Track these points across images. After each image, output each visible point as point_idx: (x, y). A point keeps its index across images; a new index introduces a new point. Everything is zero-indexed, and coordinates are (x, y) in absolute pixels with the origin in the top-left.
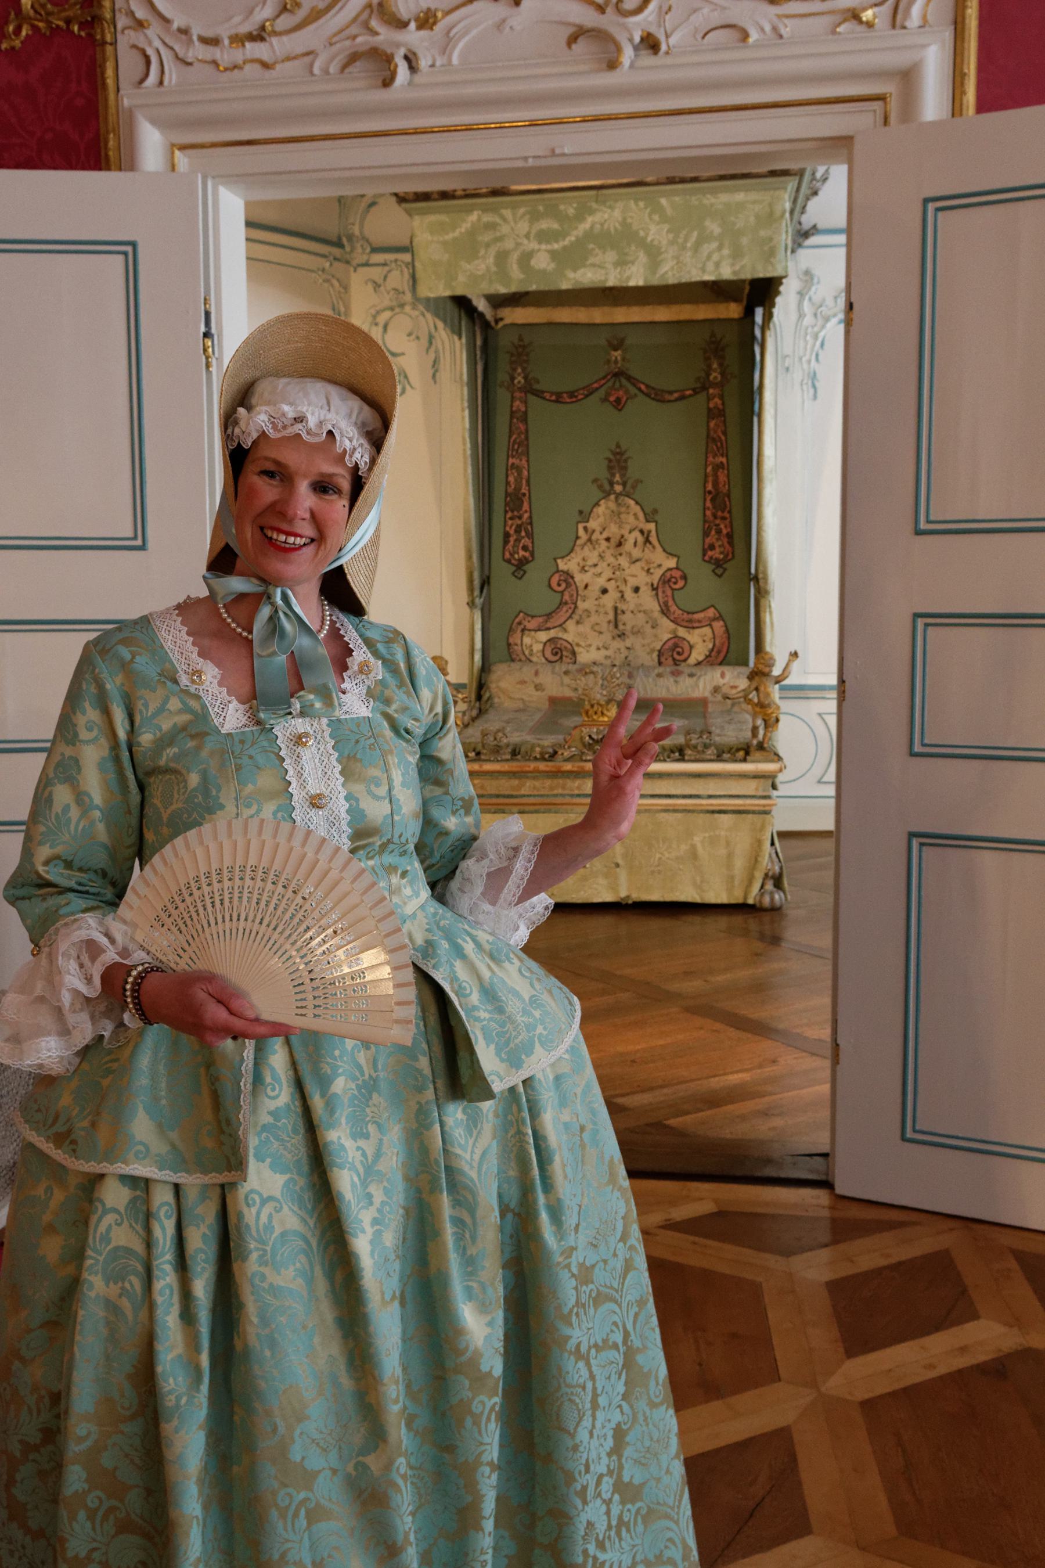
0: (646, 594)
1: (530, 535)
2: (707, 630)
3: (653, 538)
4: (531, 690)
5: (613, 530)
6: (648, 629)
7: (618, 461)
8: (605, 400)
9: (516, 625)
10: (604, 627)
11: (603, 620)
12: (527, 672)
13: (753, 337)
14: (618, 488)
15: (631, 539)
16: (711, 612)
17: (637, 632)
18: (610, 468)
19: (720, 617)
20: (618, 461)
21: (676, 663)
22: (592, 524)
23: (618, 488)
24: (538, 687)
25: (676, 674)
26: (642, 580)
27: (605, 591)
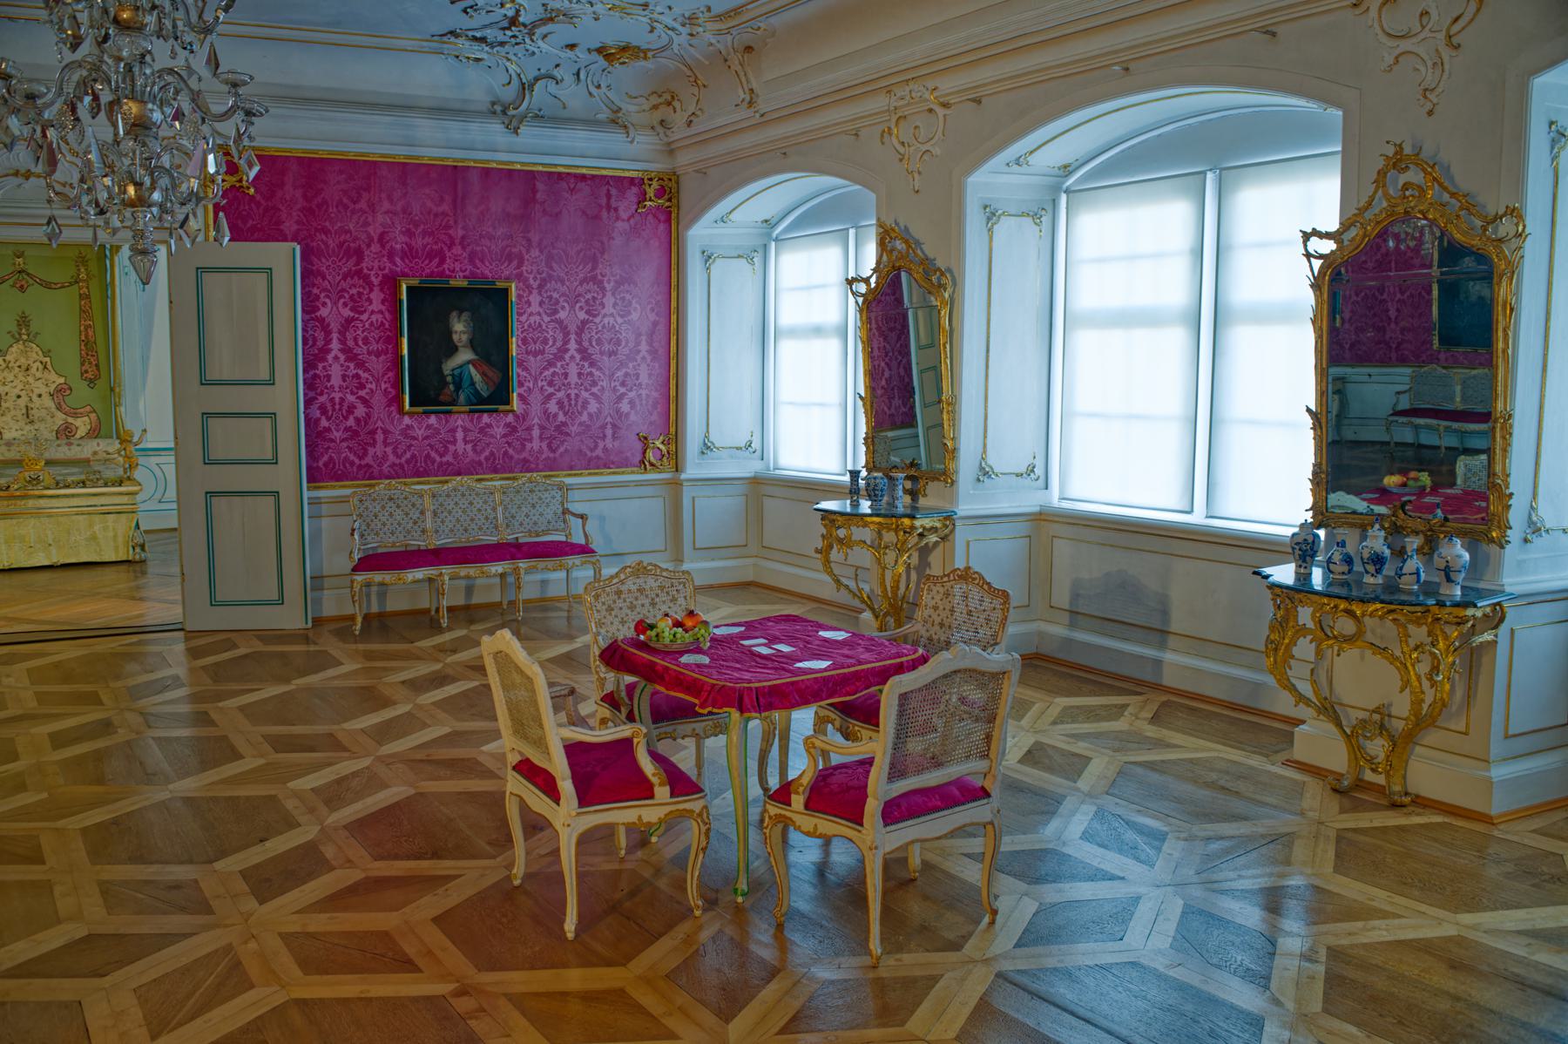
3: (49, 366)
7: (23, 321)
10: (20, 417)
11: (19, 414)
15: (35, 366)
16: (88, 408)
17: (42, 420)
19: (94, 411)
20: (23, 321)
21: (67, 437)
23: (25, 337)
25: (69, 444)
27: (19, 397)
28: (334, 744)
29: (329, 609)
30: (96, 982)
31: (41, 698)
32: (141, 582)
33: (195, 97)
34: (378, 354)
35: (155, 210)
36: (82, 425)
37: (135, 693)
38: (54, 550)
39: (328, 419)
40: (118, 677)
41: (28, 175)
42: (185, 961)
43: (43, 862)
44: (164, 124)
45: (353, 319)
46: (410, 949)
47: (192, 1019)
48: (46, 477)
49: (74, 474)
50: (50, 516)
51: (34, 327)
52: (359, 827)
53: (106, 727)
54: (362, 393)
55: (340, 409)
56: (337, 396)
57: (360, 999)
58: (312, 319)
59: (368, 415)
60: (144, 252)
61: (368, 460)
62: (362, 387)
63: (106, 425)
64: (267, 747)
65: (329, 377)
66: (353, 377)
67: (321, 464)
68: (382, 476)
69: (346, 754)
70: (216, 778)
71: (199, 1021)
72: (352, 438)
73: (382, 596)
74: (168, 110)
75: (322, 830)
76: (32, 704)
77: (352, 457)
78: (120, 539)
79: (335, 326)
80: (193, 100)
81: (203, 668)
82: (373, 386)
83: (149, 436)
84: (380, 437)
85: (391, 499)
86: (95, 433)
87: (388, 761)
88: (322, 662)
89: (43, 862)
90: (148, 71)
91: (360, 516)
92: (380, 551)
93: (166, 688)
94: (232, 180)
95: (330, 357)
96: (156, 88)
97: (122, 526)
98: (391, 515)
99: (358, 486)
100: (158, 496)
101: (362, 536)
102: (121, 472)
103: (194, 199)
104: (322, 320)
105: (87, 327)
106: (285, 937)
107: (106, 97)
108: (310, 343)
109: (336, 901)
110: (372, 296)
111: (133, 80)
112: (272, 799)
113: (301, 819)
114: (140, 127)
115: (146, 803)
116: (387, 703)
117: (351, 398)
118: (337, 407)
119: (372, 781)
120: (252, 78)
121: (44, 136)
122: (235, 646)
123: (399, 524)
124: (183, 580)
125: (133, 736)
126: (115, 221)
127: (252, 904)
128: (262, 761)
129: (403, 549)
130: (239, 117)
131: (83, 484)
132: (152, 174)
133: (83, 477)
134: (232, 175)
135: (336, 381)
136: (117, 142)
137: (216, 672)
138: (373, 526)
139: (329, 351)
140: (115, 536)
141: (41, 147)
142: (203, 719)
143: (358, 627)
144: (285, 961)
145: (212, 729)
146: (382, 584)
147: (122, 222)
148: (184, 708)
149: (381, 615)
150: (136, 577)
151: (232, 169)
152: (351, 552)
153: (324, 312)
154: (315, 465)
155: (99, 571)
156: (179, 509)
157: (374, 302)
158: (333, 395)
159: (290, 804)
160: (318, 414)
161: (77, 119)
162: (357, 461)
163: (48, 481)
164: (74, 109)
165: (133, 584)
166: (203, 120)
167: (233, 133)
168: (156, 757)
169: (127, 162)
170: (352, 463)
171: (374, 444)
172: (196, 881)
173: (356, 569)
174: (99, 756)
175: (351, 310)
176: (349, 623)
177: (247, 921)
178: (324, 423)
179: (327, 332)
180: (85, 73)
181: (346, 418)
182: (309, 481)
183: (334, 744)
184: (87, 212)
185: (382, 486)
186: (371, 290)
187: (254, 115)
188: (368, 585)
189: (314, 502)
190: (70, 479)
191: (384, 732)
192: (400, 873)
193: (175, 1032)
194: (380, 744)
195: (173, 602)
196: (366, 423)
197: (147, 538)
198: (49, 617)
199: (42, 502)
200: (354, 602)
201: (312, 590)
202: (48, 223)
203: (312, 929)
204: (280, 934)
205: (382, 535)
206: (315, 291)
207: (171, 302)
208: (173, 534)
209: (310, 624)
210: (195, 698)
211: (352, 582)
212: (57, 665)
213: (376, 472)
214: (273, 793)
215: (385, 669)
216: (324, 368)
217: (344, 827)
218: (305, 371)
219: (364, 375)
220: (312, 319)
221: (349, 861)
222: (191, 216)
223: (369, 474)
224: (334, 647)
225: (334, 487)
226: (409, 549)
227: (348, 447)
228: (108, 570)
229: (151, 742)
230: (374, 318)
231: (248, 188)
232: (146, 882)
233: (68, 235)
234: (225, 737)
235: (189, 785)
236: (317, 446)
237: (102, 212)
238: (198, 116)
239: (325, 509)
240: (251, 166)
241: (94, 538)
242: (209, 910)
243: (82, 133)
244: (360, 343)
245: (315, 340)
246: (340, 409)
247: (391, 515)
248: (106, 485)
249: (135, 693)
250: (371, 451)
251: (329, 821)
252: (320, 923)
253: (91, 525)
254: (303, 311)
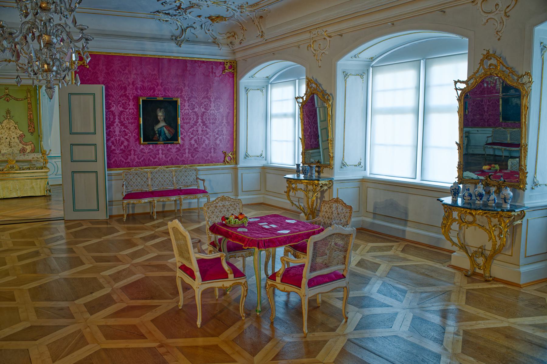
3: (17, 128)
7: (8, 112)
10: (7, 145)
11: (7, 144)
15: (12, 128)
16: (31, 142)
17: (15, 146)
19: (33, 143)
20: (8, 112)
21: (24, 152)
23: (9, 118)
25: (24, 155)
27: (7, 138)
28: (117, 259)
29: (115, 212)
30: (34, 342)
31: (14, 243)
32: (49, 203)
33: (68, 34)
34: (132, 123)
35: (54, 73)
36: (29, 148)
37: (47, 242)
38: (19, 192)
39: (115, 146)
40: (41, 236)
41: (10, 61)
42: (64, 335)
43: (15, 301)
44: (57, 43)
45: (123, 111)
46: (143, 331)
47: (67, 355)
48: (16, 166)
49: (26, 165)
50: (17, 180)
51: (12, 114)
52: (125, 288)
53: (37, 253)
54: (126, 137)
55: (119, 143)
56: (118, 138)
57: (126, 348)
58: (109, 111)
59: (129, 145)
60: (50, 88)
61: (129, 160)
62: (126, 135)
63: (37, 148)
64: (93, 261)
65: (115, 132)
66: (123, 131)
67: (112, 162)
68: (133, 166)
69: (121, 263)
70: (75, 271)
71: (69, 356)
72: (123, 153)
73: (133, 208)
74: (59, 39)
75: (112, 289)
76: (11, 245)
77: (123, 159)
78: (42, 188)
79: (117, 114)
80: (67, 35)
81: (71, 233)
82: (130, 135)
83: (52, 152)
84: (132, 152)
85: (136, 174)
86: (33, 151)
87: (135, 265)
88: (112, 231)
89: (15, 301)
90: (52, 25)
91: (126, 180)
92: (133, 192)
93: (58, 240)
94: (81, 63)
95: (115, 124)
96: (54, 31)
97: (43, 183)
98: (136, 179)
99: (125, 170)
100: (55, 173)
101: (126, 187)
102: (42, 164)
103: (68, 70)
104: (112, 112)
105: (30, 114)
106: (99, 327)
107: (37, 34)
108: (108, 119)
109: (117, 314)
110: (130, 103)
111: (46, 28)
112: (95, 278)
113: (105, 286)
114: (49, 44)
115: (51, 280)
116: (135, 245)
117: (123, 139)
118: (118, 142)
119: (130, 272)
120: (88, 27)
121: (16, 47)
122: (82, 225)
123: (139, 183)
124: (64, 202)
125: (47, 257)
126: (40, 77)
127: (88, 315)
128: (91, 265)
129: (141, 191)
130: (83, 41)
131: (29, 169)
132: (53, 61)
133: (29, 166)
134: (81, 61)
135: (117, 133)
136: (41, 50)
137: (75, 234)
138: (130, 183)
139: (115, 122)
140: (40, 187)
141: (14, 51)
142: (71, 251)
143: (125, 218)
144: (99, 335)
145: (74, 254)
146: (133, 204)
147: (43, 77)
148: (64, 247)
149: (133, 215)
150: (48, 201)
151: (81, 59)
152: (122, 193)
153: (113, 109)
154: (110, 162)
155: (35, 199)
156: (62, 177)
157: (131, 105)
158: (116, 138)
159: (101, 280)
160: (111, 144)
161: (27, 42)
162: (125, 161)
163: (17, 168)
164: (26, 38)
165: (46, 204)
166: (71, 42)
167: (81, 46)
168: (54, 264)
169: (44, 56)
170: (123, 162)
171: (130, 155)
172: (68, 307)
173: (124, 198)
174: (34, 264)
175: (123, 108)
176: (122, 217)
177: (86, 321)
178: (113, 147)
179: (114, 116)
180: (30, 25)
181: (121, 146)
182: (108, 168)
183: (117, 259)
184: (30, 74)
185: (133, 170)
186: (130, 101)
187: (89, 40)
188: (128, 204)
189: (110, 175)
190: (24, 167)
191: (134, 255)
192: (140, 305)
193: (61, 360)
194: (133, 259)
195: (60, 210)
196: (128, 148)
197: (51, 187)
198: (17, 215)
199: (15, 175)
200: (123, 210)
201: (109, 206)
202: (17, 78)
203: (109, 324)
204: (98, 326)
205: (133, 186)
206: (110, 101)
207: (60, 105)
208: (61, 186)
209: (108, 218)
210: (68, 243)
211: (123, 203)
212: (20, 232)
213: (131, 164)
214: (95, 276)
215: (134, 233)
216: (113, 128)
217: (120, 288)
218: (106, 129)
219: (127, 131)
220: (109, 111)
221: (122, 300)
222: (67, 75)
223: (129, 165)
224: (116, 226)
225: (116, 170)
226: (143, 191)
227: (121, 156)
228: (38, 199)
229: (53, 259)
230: (130, 111)
231: (87, 66)
232: (51, 308)
233: (24, 82)
234: (79, 257)
235: (66, 274)
236: (111, 155)
237: (36, 74)
238: (69, 40)
239: (113, 177)
240: (87, 58)
241: (33, 188)
242: (73, 317)
243: (29, 46)
244: (126, 119)
245: (110, 118)
246: (119, 143)
247: (136, 179)
248: (37, 169)
249: (47, 242)
250: (129, 157)
251: (115, 286)
252: (112, 322)
253: (32, 183)
254: (106, 108)
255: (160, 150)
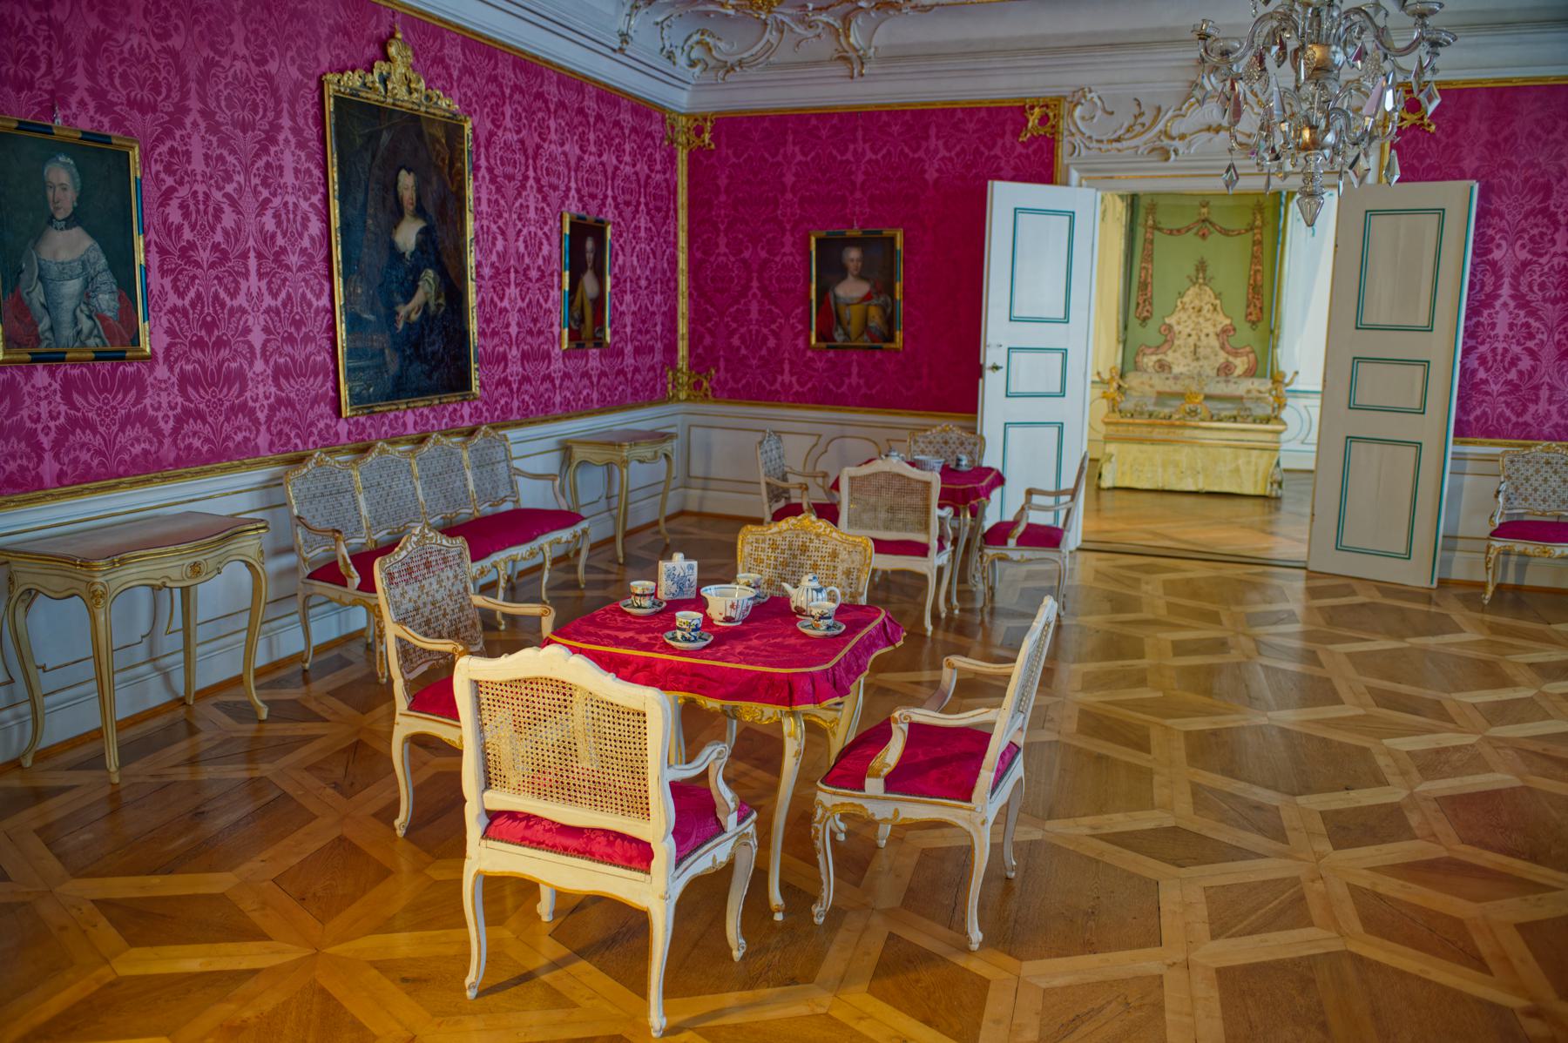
0: (1212, 336)
1: (1150, 304)
2: (1245, 359)
3: (1219, 308)
4: (1147, 388)
5: (1197, 303)
6: (1213, 357)
7: (1201, 267)
8: (1196, 234)
9: (1140, 352)
10: (1188, 354)
11: (1188, 350)
12: (1145, 377)
13: (1281, 203)
14: (1201, 281)
15: (1206, 308)
16: (1248, 349)
17: (1206, 358)
18: (1197, 270)
19: (1253, 352)
20: (1201, 267)
21: (1227, 375)
22: (1186, 299)
23: (1201, 281)
24: (1151, 386)
25: (1227, 381)
26: (1211, 330)
27: (1190, 335)
28: (1439, 712)
29: (1459, 572)
30: (1172, 869)
31: (1172, 607)
32: (1273, 517)
33: (1381, 34)
34: (1555, 301)
35: (1327, 152)
36: (1241, 364)
37: (1253, 620)
38: (1201, 477)
39: (1487, 370)
40: (1239, 602)
41: (1218, 130)
42: (1253, 878)
43: (1148, 751)
44: (1346, 65)
45: (1530, 263)
46: (1484, 946)
47: (1250, 933)
48: (1203, 409)
49: (1228, 409)
50: (1202, 446)
51: (1209, 273)
52: (1455, 805)
53: (1220, 646)
54: (1530, 344)
55: (1502, 361)
56: (1500, 346)
57: (1419, 978)
58: (1483, 262)
59: (1534, 369)
60: (1312, 195)
61: (1528, 418)
62: (1531, 336)
63: (1264, 366)
64: (1368, 699)
65: (1493, 326)
66: (1522, 325)
67: (1471, 418)
68: (1541, 436)
69: (1451, 726)
70: (1312, 717)
71: (1256, 938)
72: (1511, 393)
73: (1521, 568)
74: (1350, 51)
75: (1411, 796)
76: (1162, 612)
77: (1508, 413)
78: (1260, 474)
79: (1508, 270)
80: (1377, 37)
81: (1320, 608)
82: (1545, 337)
83: (1300, 378)
84: (1544, 393)
85: (1548, 463)
86: (1251, 373)
87: (1499, 744)
88: (1441, 625)
89: (1148, 751)
90: (1335, 14)
91: (1509, 477)
92: (1526, 518)
93: (1279, 621)
94: (1412, 118)
95: (1498, 304)
96: (1342, 29)
97: (1263, 461)
98: (1546, 480)
99: (1511, 445)
100: (1302, 437)
101: (1508, 499)
102: (1269, 411)
103: (1367, 139)
104: (1493, 264)
105: (1257, 271)
106: (1354, 890)
107: (1292, 45)
108: (1478, 287)
109: (1413, 871)
110: (1557, 236)
111: (1319, 25)
112: (1364, 751)
113: (1390, 779)
114: (1322, 70)
115: (1244, 723)
116: (1504, 682)
117: (1516, 349)
118: (1499, 358)
119: (1476, 762)
120: (1441, 5)
121: (1233, 88)
122: (1353, 593)
123: (1554, 492)
124: (1312, 520)
125: (1245, 659)
126: (1288, 167)
127: (1325, 846)
128: (1361, 712)
129: (1554, 520)
130: (1424, 48)
131: (1235, 419)
132: (1327, 117)
133: (1235, 413)
134: (1413, 113)
135: (1502, 329)
136: (1298, 88)
137: (1332, 615)
138: (1522, 490)
139: (1498, 296)
140: (1257, 471)
141: (1229, 99)
142: (1311, 657)
143: (1488, 596)
144: (1348, 913)
145: (1318, 669)
146: (1522, 555)
147: (1294, 166)
148: (1297, 644)
149: (1517, 589)
150: (1270, 512)
151: (1413, 106)
152: (1492, 516)
153: (1497, 255)
154: (1465, 418)
155: (1237, 501)
156: (1318, 452)
157: (1558, 243)
158: (1496, 345)
159: (1382, 761)
160: (1476, 364)
161: (1264, 70)
162: (1514, 419)
163: (1204, 414)
164: (1261, 60)
165: (1267, 518)
166: (1386, 57)
167: (1414, 67)
168: (1261, 684)
169: (1305, 106)
170: (1508, 420)
171: (1536, 401)
172: (1277, 808)
173: (1495, 534)
174: (1211, 671)
175: (1530, 252)
176: (1476, 590)
177: (1318, 860)
178: (1482, 374)
179: (1499, 277)
180: (1275, 24)
181: (1507, 371)
182: (1456, 434)
183: (1439, 712)
184: (1263, 159)
185: (1539, 448)
186: (1557, 230)
187: (1441, 45)
188: (1507, 553)
189: (1458, 457)
190: (1224, 414)
191: (1499, 713)
192: (1489, 865)
193: (1233, 939)
194: (1491, 724)
195: (1299, 541)
196: (1530, 378)
197: (1286, 476)
198: (1185, 537)
199: (1197, 433)
200: (1487, 569)
201: (1443, 549)
202: (1227, 171)
203: (1381, 890)
204: (1348, 884)
205: (1531, 500)
206: (1490, 232)
207: (1336, 246)
208: (1310, 476)
209: (1435, 585)
210: (1307, 636)
211: (1489, 547)
212: (1189, 581)
213: (1534, 431)
214: (1367, 745)
215: (1511, 646)
216: (1490, 315)
217: (1436, 799)
218: (1468, 318)
219: (1535, 324)
220: (1483, 262)
221: (1434, 835)
222: (1362, 156)
223: (1526, 433)
224: (1457, 613)
225: (1482, 444)
226: (1562, 520)
227: (1505, 402)
228: (1245, 502)
229: (1259, 668)
230: (1556, 261)
231: (1429, 125)
232: (1233, 795)
233: (1244, 184)
234: (1328, 680)
235: (1289, 717)
236: (1470, 399)
237: (1277, 158)
238: (1381, 53)
239: (1469, 466)
240: (1430, 100)
241: (1237, 470)
242: (1285, 840)
243: (1267, 83)
244: (1536, 288)
245: (1483, 285)
246: (1502, 361)
247: (1546, 480)
248: (1254, 422)
249: (1253, 620)
250: (1532, 408)
251: (1419, 788)
252: (1390, 887)
253: (1236, 458)
254: (1474, 253)
255: (1545, 387)
